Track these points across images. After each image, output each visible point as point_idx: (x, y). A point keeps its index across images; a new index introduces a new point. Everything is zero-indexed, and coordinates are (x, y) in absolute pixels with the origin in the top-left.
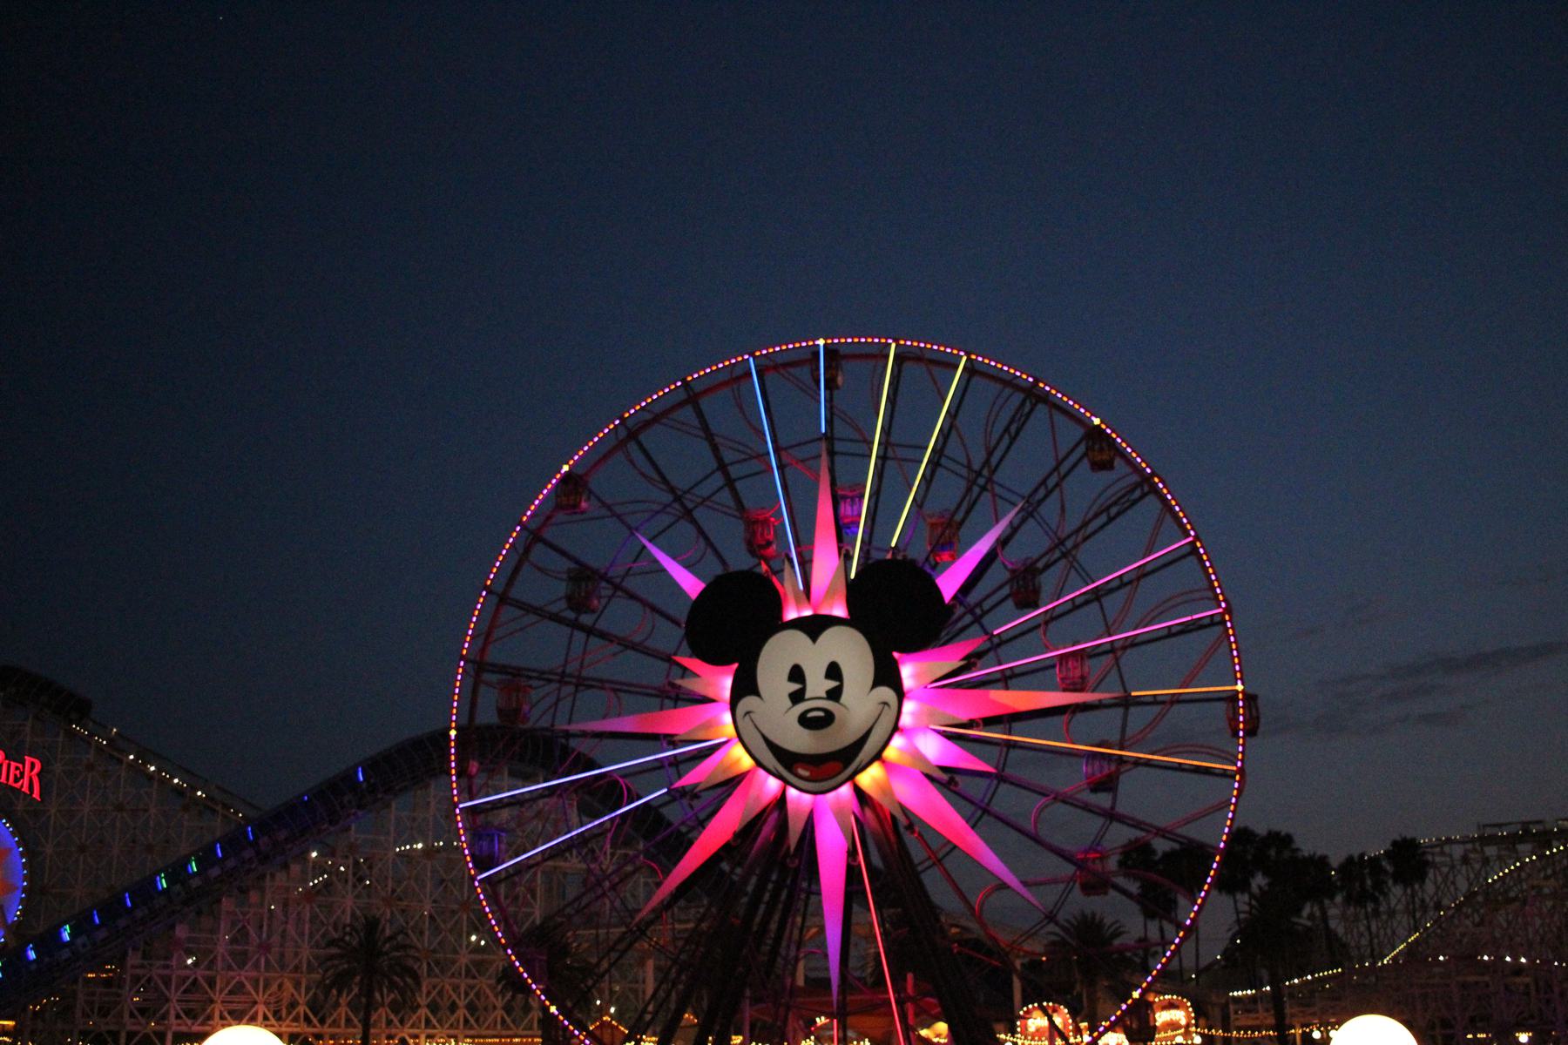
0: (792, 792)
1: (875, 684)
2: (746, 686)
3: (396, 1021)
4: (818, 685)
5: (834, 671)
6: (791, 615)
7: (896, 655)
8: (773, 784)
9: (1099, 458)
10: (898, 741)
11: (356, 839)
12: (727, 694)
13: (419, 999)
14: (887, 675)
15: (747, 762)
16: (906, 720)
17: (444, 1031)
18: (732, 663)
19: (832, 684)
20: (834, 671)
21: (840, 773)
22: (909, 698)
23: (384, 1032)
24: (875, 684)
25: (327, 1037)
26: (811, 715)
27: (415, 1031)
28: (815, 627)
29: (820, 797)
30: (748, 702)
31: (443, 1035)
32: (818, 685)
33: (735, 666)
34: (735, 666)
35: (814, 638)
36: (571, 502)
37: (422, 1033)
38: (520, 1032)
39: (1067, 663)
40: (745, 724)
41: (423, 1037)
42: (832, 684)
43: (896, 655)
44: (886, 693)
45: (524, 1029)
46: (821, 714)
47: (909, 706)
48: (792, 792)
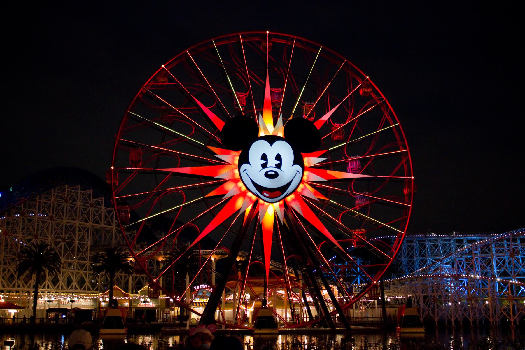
0: (261, 201)
1: (294, 163)
2: (244, 159)
3: (6, 285)
4: (272, 162)
5: (278, 157)
6: (262, 134)
7: (301, 153)
8: (254, 198)
9: (366, 91)
10: (301, 186)
11: (24, 210)
12: (236, 162)
13: (59, 277)
14: (298, 161)
15: (244, 188)
16: (305, 178)
17: (54, 290)
18: (240, 150)
19: (279, 162)
20: (278, 157)
21: (280, 196)
22: (306, 171)
23: (32, 290)
24: (294, 163)
25: (5, 292)
26: (269, 173)
27: (44, 290)
28: (271, 139)
29: (271, 204)
30: (244, 166)
31: (53, 292)
32: (272, 162)
33: (240, 152)
34: (240, 152)
35: (271, 144)
36: (163, 80)
37: (46, 291)
38: (81, 291)
39: (353, 163)
40: (244, 175)
41: (47, 292)
42: (279, 162)
43: (301, 153)
44: (298, 167)
45: (83, 290)
46: (274, 173)
47: (306, 173)
48: (261, 201)
